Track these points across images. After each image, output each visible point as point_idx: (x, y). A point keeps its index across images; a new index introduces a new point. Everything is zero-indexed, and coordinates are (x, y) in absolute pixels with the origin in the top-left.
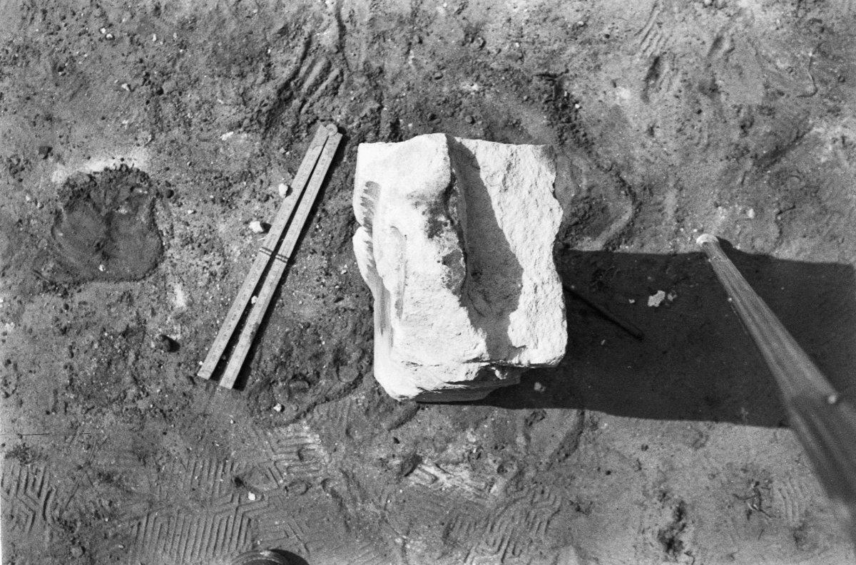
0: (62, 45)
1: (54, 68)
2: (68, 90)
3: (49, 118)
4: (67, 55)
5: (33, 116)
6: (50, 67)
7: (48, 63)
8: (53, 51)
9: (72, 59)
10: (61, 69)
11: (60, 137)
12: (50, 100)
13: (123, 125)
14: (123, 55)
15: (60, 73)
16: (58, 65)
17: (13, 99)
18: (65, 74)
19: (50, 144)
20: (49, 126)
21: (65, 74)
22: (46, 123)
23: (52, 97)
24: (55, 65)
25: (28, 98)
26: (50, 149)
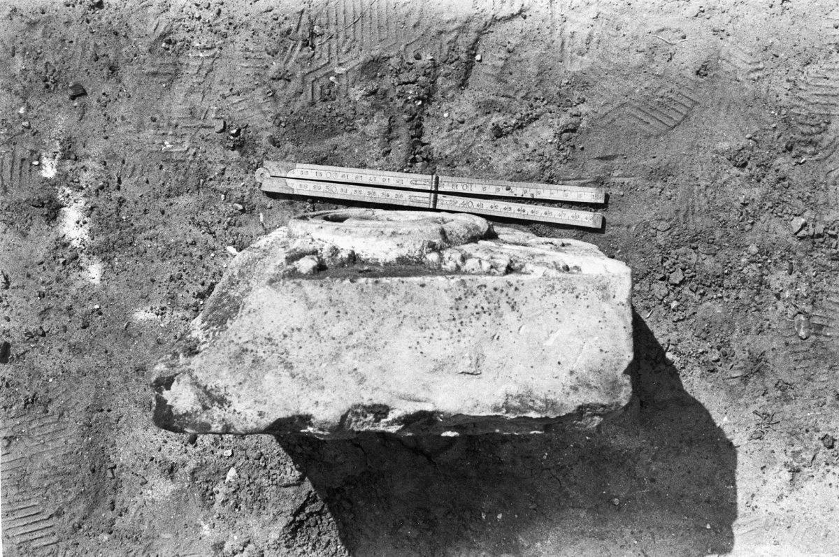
0: (195, 23)
1: (163, 36)
2: (153, 66)
3: (113, 69)
4: (188, 36)
5: (102, 52)
6: (161, 30)
7: (164, 25)
8: (180, 20)
9: (188, 45)
10: (169, 42)
11: (104, 94)
12: (132, 56)
13: (163, 144)
14: (231, 90)
15: (164, 45)
16: (171, 36)
17: (103, 20)
18: (168, 49)
19: (89, 90)
20: (105, 75)
21: (168, 49)
22: (105, 71)
23: (135, 56)
24: (170, 33)
25: (116, 34)
26: (84, 93)
